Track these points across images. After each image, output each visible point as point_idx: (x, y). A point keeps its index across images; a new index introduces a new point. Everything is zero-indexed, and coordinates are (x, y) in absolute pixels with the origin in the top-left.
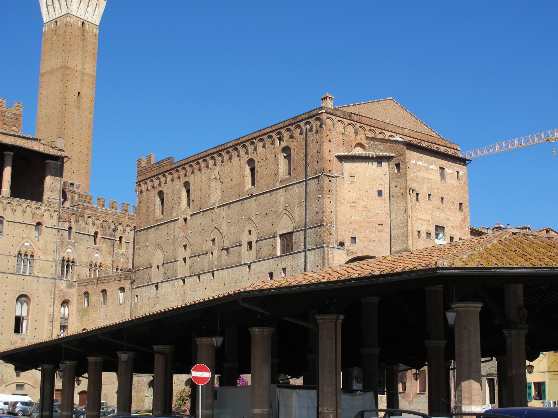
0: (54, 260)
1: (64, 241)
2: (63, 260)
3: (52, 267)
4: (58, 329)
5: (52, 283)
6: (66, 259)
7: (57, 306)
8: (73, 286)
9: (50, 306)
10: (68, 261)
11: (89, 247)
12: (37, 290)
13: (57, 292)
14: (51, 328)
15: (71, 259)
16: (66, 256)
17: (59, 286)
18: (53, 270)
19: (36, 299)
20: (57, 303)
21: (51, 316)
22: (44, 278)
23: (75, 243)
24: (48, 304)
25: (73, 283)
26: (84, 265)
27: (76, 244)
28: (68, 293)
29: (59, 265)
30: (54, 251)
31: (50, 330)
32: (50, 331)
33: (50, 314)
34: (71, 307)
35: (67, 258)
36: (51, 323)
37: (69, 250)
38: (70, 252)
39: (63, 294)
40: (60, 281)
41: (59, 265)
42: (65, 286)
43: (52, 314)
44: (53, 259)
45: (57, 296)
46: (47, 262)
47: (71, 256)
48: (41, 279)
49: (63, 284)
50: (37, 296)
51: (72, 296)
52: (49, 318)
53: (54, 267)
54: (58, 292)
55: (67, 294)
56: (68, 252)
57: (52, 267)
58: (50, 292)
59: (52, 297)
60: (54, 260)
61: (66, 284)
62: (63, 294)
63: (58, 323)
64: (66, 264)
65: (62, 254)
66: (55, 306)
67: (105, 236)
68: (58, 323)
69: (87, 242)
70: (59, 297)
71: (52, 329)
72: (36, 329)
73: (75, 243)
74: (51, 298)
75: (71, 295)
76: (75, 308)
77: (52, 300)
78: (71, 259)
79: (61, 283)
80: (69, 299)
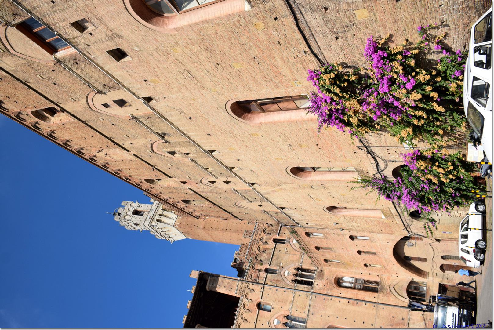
0: (294, 293)
1: (276, 279)
2: (295, 281)
3: (300, 295)
4: (365, 294)
5: (315, 297)
6: (294, 278)
7: (341, 293)
8: (322, 271)
9: (340, 302)
10: (296, 275)
11: (285, 250)
12: (321, 316)
13: (326, 292)
14: (364, 303)
15: (295, 272)
16: (291, 278)
17: (319, 289)
18: (303, 294)
19: (331, 318)
20: (337, 293)
21: (351, 301)
22: (310, 306)
23: (279, 266)
24: (338, 304)
25: (319, 271)
26: (303, 256)
27: (281, 264)
28: (328, 278)
29: (298, 287)
30: (285, 291)
31: (366, 304)
32: (367, 304)
33: (349, 302)
34: (343, 275)
35: (293, 276)
36: (359, 302)
37: (286, 274)
38: (288, 273)
39: (329, 285)
40: (315, 287)
41: (298, 287)
42: (320, 282)
43: (348, 300)
44: (292, 293)
45: (330, 293)
46: (295, 300)
47: (292, 271)
48: (311, 310)
49: (318, 284)
50: (328, 317)
51: (332, 274)
52: (353, 304)
53: (300, 293)
54: (326, 290)
55: (329, 279)
56: (288, 276)
57: (300, 295)
58: (325, 301)
59: (330, 299)
60: (294, 293)
61: (318, 280)
62: (329, 285)
63: (358, 293)
64: (299, 278)
65: (288, 283)
66: (340, 295)
67: (278, 230)
68: (358, 293)
69: (280, 252)
70: (331, 289)
71: (365, 301)
72: (363, 323)
73: (279, 266)
74: (331, 299)
75: (331, 274)
76: (344, 270)
77: (333, 298)
78: (295, 272)
79: (317, 286)
80: (334, 278)
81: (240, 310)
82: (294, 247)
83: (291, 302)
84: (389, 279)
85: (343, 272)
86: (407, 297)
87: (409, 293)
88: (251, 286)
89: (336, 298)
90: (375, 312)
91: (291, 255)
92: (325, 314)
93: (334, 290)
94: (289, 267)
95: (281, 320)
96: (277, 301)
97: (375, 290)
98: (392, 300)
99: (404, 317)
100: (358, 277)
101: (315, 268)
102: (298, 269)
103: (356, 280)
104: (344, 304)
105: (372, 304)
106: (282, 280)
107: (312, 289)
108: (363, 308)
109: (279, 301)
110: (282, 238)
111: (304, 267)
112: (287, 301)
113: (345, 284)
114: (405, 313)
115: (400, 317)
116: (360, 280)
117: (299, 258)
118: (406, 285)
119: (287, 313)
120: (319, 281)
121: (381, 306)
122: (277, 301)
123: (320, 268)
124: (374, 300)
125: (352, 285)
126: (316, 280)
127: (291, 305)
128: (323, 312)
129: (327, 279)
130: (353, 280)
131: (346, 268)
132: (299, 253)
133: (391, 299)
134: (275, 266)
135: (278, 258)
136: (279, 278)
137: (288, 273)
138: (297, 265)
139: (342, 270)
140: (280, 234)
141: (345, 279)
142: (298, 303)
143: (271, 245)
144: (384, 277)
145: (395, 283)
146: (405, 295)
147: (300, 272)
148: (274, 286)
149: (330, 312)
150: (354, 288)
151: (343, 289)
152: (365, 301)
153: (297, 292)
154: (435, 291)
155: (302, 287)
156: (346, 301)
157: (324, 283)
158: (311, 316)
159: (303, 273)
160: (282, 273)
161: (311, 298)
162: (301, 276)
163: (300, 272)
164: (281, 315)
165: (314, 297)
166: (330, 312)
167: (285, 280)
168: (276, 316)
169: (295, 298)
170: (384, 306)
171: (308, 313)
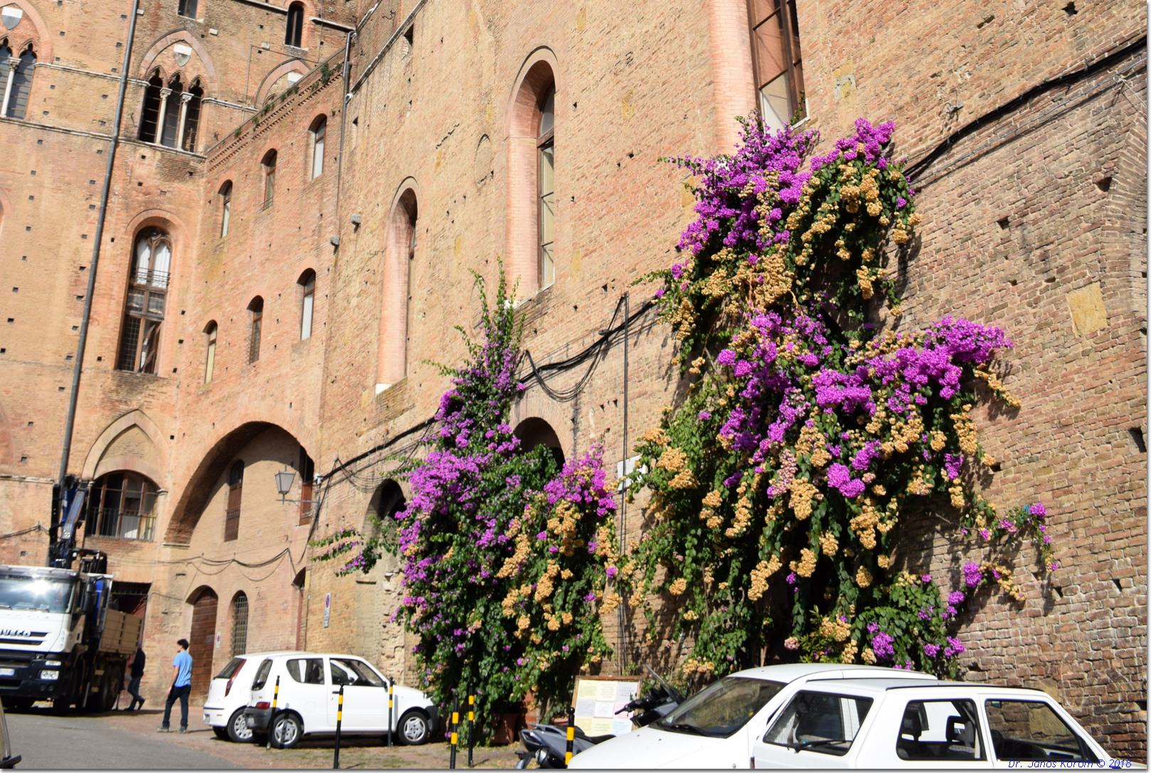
0: (114, 75)
1: (162, 13)
2: (156, 82)
3: (105, 96)
4: (111, 326)
5: (99, 151)
6: (167, 75)
7: (113, 240)
8: (191, 174)
9: (84, 236)
10: (176, 85)
11: (263, 45)
12: (33, 173)
13: (116, 187)
14: (79, 322)
15: (188, 78)
16: (165, 67)
17: (127, 166)
18: (109, 109)
19: (26, 205)
20: (112, 226)
21: (86, 276)
22: (67, 132)
23: (208, 25)
24: (75, 232)
25: (192, 164)
26: (245, 106)
27: (214, 31)
28: (168, 195)
29: (136, 92)
30: (119, 45)
31: (75, 328)
32: (76, 332)
33: (82, 268)
34: (178, 247)
35: (172, 72)
36: (81, 305)
37: (179, 48)
38: (184, 56)
39: (141, 198)
40: (135, 150)
41: (136, 92)
42: (154, 170)
43: (89, 266)
44: (114, 70)
45: (114, 201)
46: (88, 78)
47: (190, 69)
48: (53, 138)
49: (146, 161)
50: (31, 198)
51: (182, 209)
52: (77, 282)
53: (114, 99)
54: (124, 189)
55: (161, 198)
56: (174, 55)
57: (105, 96)
58: (87, 184)
59: (93, 203)
60: (114, 75)
61: (160, 161)
62: (141, 198)
63: (113, 302)
64: (165, 93)
65: (150, 56)
66: (106, 237)
67: (333, 19)
68: (113, 302)
69: (258, 29)
70: (127, 207)
71: (86, 325)
72: (11, 320)
73: (208, 25)
74: (92, 207)
75: (180, 204)
76: (194, 253)
77: (95, 215)
78: (188, 78)
79: (138, 156)
80: (168, 216)
82: (274, 76)
83: (84, 66)
84: (164, 408)
85: (186, 247)
86: (102, 470)
87: (114, 479)
89: (96, 225)
90: (49, 359)
91: (246, 64)
92: (41, 186)
93: (123, 215)
94: (206, 58)
95: (20, 31)
96: (85, 18)
97: (124, 359)
98: (89, 419)
99: (31, 463)
100: (171, 301)
101: (200, 148)
102: (197, 90)
103: (161, 294)
104: (77, 251)
105: (74, 349)
106: (158, 35)
107: (128, 139)
108: (63, 316)
109: (84, 25)
110: (305, 33)
111: (206, 111)
112: (86, 51)
113: (145, 255)
114: (44, 466)
115: (30, 449)
116: (162, 308)
118: (141, 467)
119: (42, 51)
121: (69, 382)
122: (85, 18)
123: (200, 166)
124: (89, 357)
125: (141, 281)
126: (158, 155)
127: (72, 67)
128: (47, 178)
129: (163, 193)
130: (158, 284)
131: (202, 258)
132: (252, 94)
133: (94, 417)
134: (208, 9)
135: (236, 19)
136: (165, 25)
138: (211, 88)
139: (196, 243)
141: (163, 257)
142: (77, 89)
144: (172, 390)
145: (151, 428)
146: (108, 466)
147: (187, 96)
148: (138, 7)
149: (49, 202)
150: (131, 288)
151: (129, 248)
152: (86, 325)
153: (118, 87)
154: (123, 569)
155: (136, 104)
156: (87, 258)
157: (153, 181)
158: (32, 135)
159: (184, 108)
160: (184, 35)
161: (95, 137)
162: (174, 102)
163: (187, 96)
164: (36, 31)
165: (100, 145)
166: (49, 202)
167: (159, 46)
168: (32, 13)
169: (95, 80)
170: (69, 391)
171: (44, 127)
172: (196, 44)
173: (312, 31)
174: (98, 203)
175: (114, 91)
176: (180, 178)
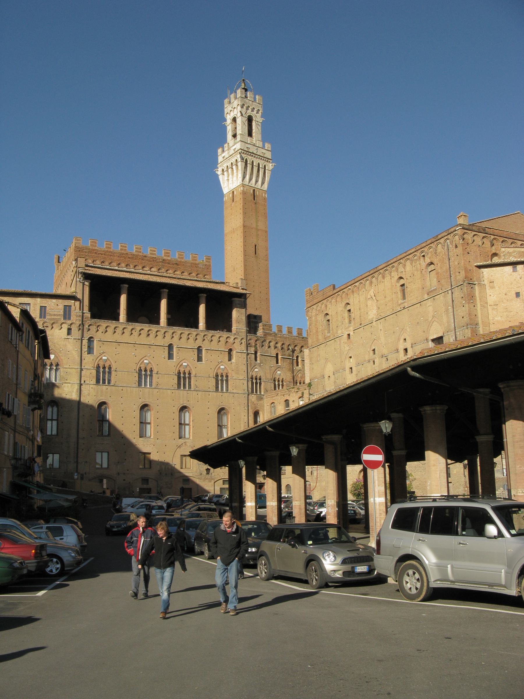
9: (245, 416)
11: (272, 366)
23: (261, 363)
27: (262, 364)
37: (256, 370)
48: (236, 395)
60: (245, 379)
70: (252, 408)
80: (259, 409)
81: (225, 334)
88: (244, 341)
89: (247, 413)
91: (269, 371)
106: (252, 368)
117: (268, 378)
120: (255, 398)
127: (236, 378)
134: (260, 359)
137: (257, 371)
138: (263, 378)
140: (283, 359)
143: (273, 352)
148: (247, 361)
153: (246, 381)
157: (255, 402)
158: (231, 395)
164: (228, 371)
167: (252, 370)
169: (241, 380)
172: (259, 368)
173: (281, 360)
174: (246, 408)
175: (245, 382)
176: (260, 400)
